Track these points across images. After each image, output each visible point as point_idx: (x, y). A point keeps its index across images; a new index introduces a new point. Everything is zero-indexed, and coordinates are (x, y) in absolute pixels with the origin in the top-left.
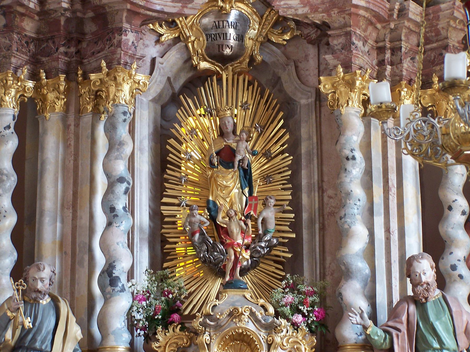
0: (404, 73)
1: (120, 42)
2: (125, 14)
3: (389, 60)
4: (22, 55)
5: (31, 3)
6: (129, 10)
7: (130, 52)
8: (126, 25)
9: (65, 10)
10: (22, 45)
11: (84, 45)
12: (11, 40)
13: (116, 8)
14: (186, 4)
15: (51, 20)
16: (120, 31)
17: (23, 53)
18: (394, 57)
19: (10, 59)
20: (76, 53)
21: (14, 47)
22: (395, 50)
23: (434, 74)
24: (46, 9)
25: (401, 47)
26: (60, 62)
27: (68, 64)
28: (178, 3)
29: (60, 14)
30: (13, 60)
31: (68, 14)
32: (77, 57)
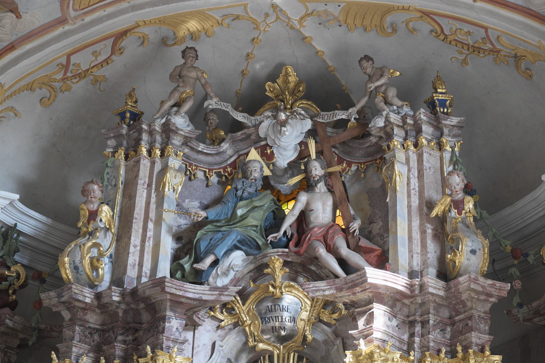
0: (432, 344)
1: (164, 329)
2: (168, 304)
3: (420, 333)
4: (83, 345)
5: (87, 298)
6: (171, 300)
7: (172, 337)
8: (169, 313)
9: (119, 302)
10: (86, 336)
11: (141, 333)
12: (74, 331)
13: (159, 299)
14: (223, 291)
15: (112, 312)
16: (164, 319)
17: (86, 343)
18: (424, 330)
19: (72, 348)
20: (133, 341)
21: (77, 337)
22: (424, 323)
23: (458, 344)
24: (101, 303)
25: (429, 320)
26: (117, 349)
27: (126, 351)
28: (215, 291)
29: (115, 307)
30: (74, 349)
31: (123, 306)
32: (133, 344)
